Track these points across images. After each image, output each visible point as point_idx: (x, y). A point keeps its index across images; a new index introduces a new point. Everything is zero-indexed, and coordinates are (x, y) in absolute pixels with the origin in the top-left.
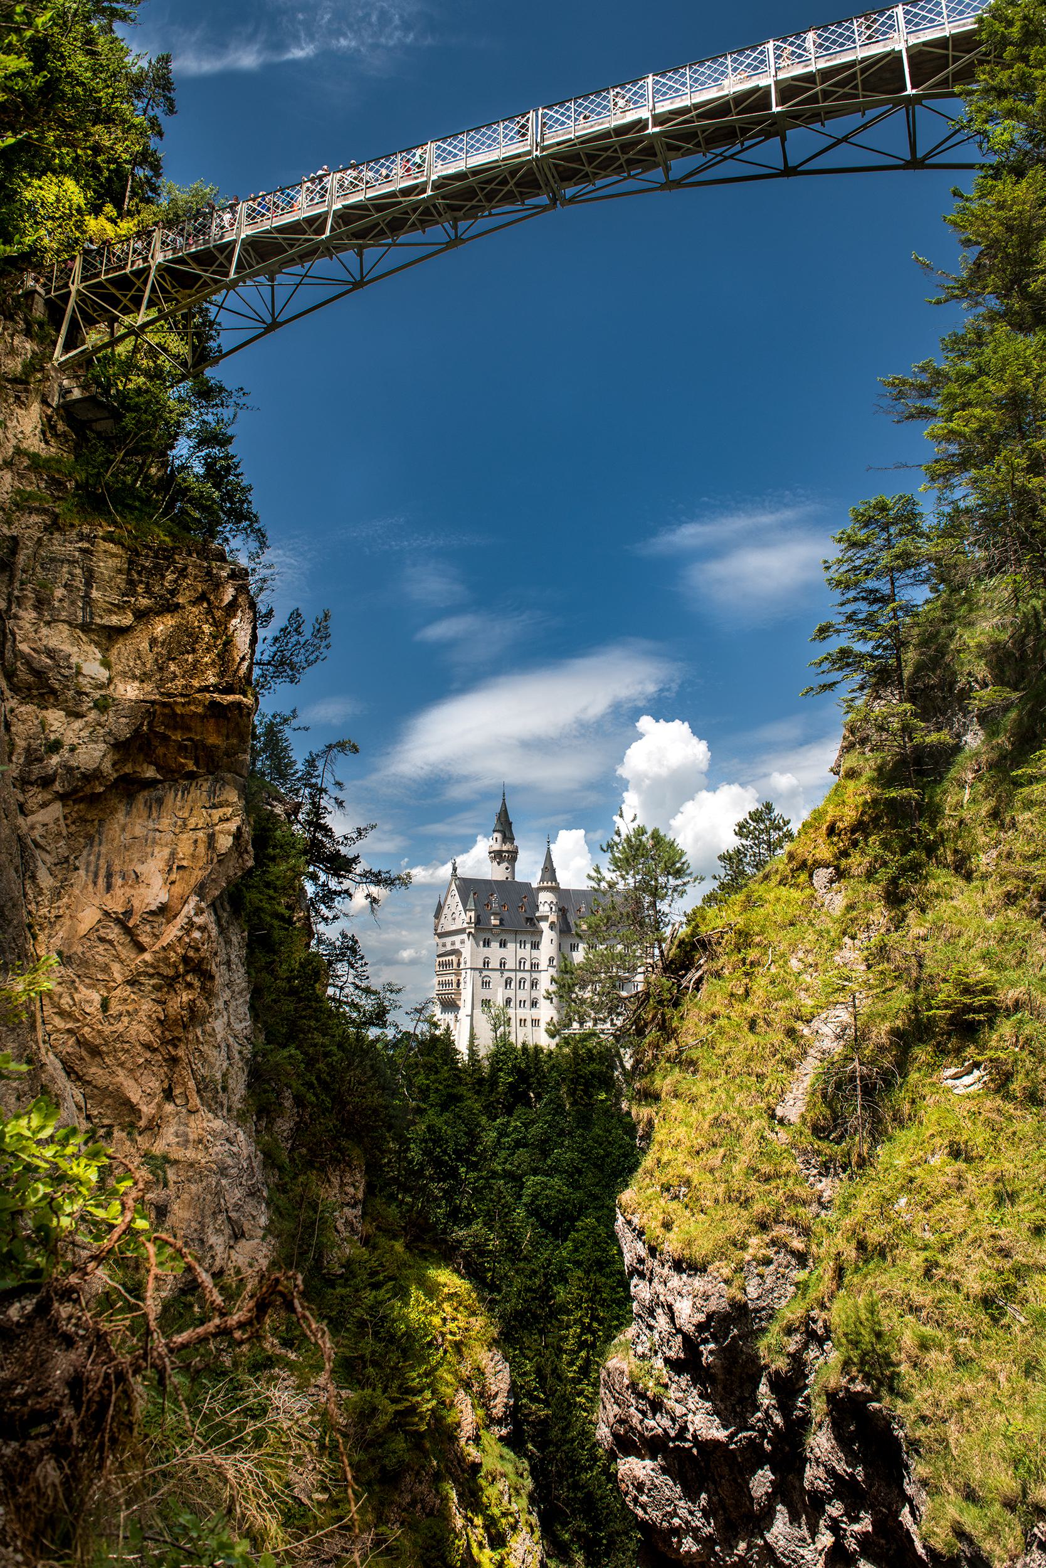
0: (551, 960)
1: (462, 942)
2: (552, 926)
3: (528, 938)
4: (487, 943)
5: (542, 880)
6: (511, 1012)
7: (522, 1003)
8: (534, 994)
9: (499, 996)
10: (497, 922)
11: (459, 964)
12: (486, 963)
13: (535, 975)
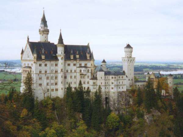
0: (62, 70)
1: (32, 64)
2: (62, 59)
3: (54, 63)
4: (40, 65)
5: (59, 43)
6: (49, 87)
7: (52, 84)
8: (56, 81)
9: (45, 82)
10: (44, 58)
11: (31, 72)
12: (40, 72)
13: (56, 74)
